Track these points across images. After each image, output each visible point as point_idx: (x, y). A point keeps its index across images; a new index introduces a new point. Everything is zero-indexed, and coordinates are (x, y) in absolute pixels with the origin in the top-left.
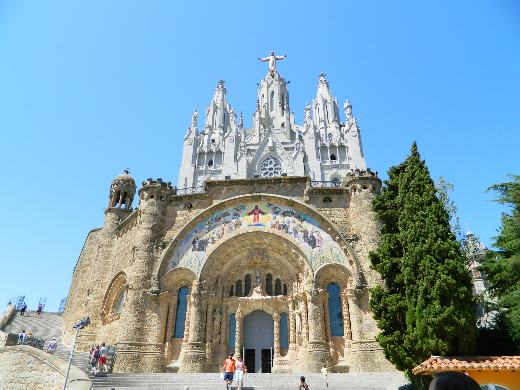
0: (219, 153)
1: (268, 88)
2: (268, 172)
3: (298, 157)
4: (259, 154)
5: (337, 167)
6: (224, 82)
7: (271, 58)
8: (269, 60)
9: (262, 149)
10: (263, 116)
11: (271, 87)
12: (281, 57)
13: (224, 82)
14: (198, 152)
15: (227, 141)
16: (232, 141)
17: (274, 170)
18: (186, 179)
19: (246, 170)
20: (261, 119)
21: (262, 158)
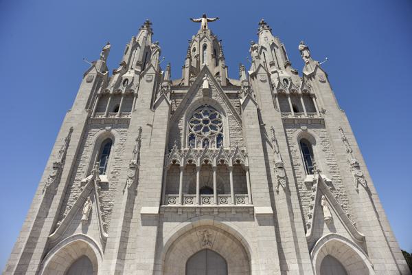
0: (131, 96)
1: (200, 41)
2: (201, 126)
3: (248, 104)
4: (189, 101)
5: (304, 122)
6: (151, 24)
7: (203, 19)
8: (201, 21)
9: (193, 93)
10: (194, 64)
11: (203, 40)
12: (212, 19)
13: (151, 24)
14: (99, 92)
15: (143, 80)
16: (149, 79)
17: (210, 123)
18: (71, 130)
19: (166, 120)
20: (191, 67)
21: (193, 106)
